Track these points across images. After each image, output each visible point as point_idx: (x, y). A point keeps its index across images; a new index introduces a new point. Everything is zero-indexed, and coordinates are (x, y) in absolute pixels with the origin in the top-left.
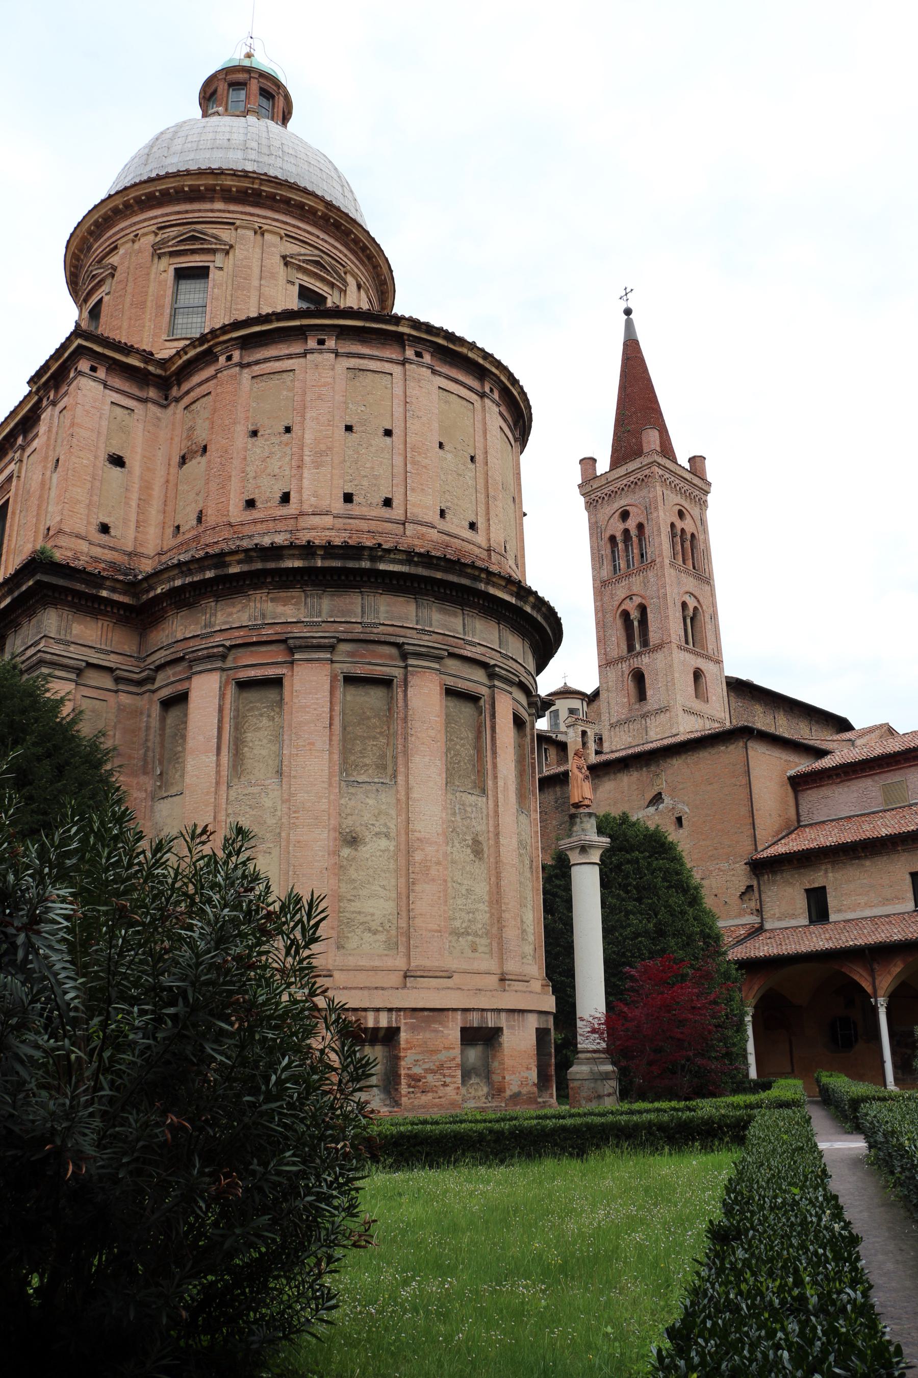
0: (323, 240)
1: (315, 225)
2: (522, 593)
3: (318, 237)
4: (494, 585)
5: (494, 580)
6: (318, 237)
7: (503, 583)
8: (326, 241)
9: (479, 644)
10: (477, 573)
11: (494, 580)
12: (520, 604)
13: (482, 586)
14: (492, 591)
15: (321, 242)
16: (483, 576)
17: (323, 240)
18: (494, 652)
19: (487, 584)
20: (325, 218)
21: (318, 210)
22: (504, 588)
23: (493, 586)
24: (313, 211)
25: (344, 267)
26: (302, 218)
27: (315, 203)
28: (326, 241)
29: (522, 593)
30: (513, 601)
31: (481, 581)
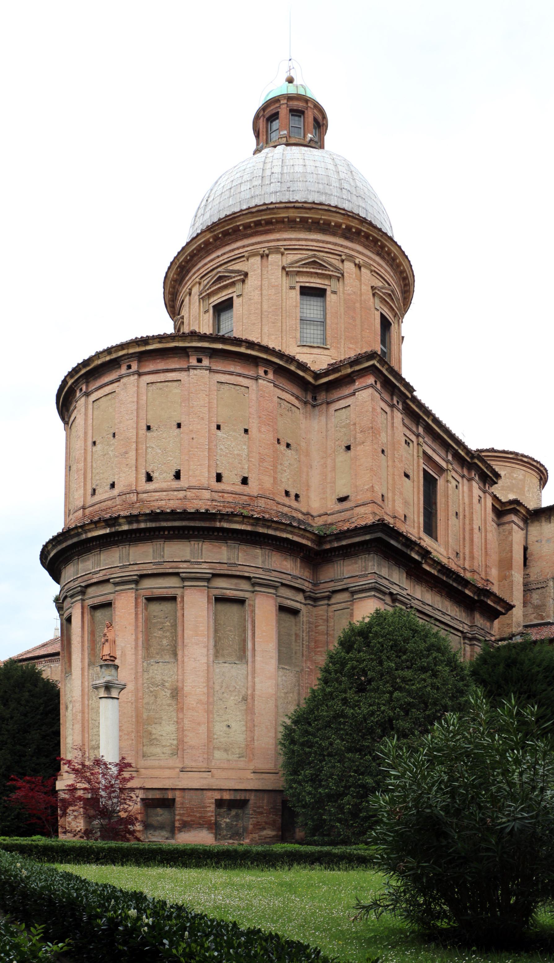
0: (222, 255)
1: (217, 248)
2: (110, 522)
3: (218, 257)
4: (90, 531)
5: (87, 528)
6: (218, 257)
7: (93, 526)
8: (224, 254)
9: (100, 570)
10: (76, 531)
11: (87, 528)
12: (113, 530)
13: (84, 537)
14: (90, 535)
15: (221, 258)
16: (80, 530)
17: (222, 255)
18: (113, 569)
19: (86, 533)
20: (216, 238)
21: (209, 239)
22: (96, 528)
23: (90, 531)
24: (207, 243)
25: (243, 256)
26: (209, 253)
27: (204, 237)
28: (224, 254)
29: (110, 522)
30: (108, 531)
31: (82, 534)
